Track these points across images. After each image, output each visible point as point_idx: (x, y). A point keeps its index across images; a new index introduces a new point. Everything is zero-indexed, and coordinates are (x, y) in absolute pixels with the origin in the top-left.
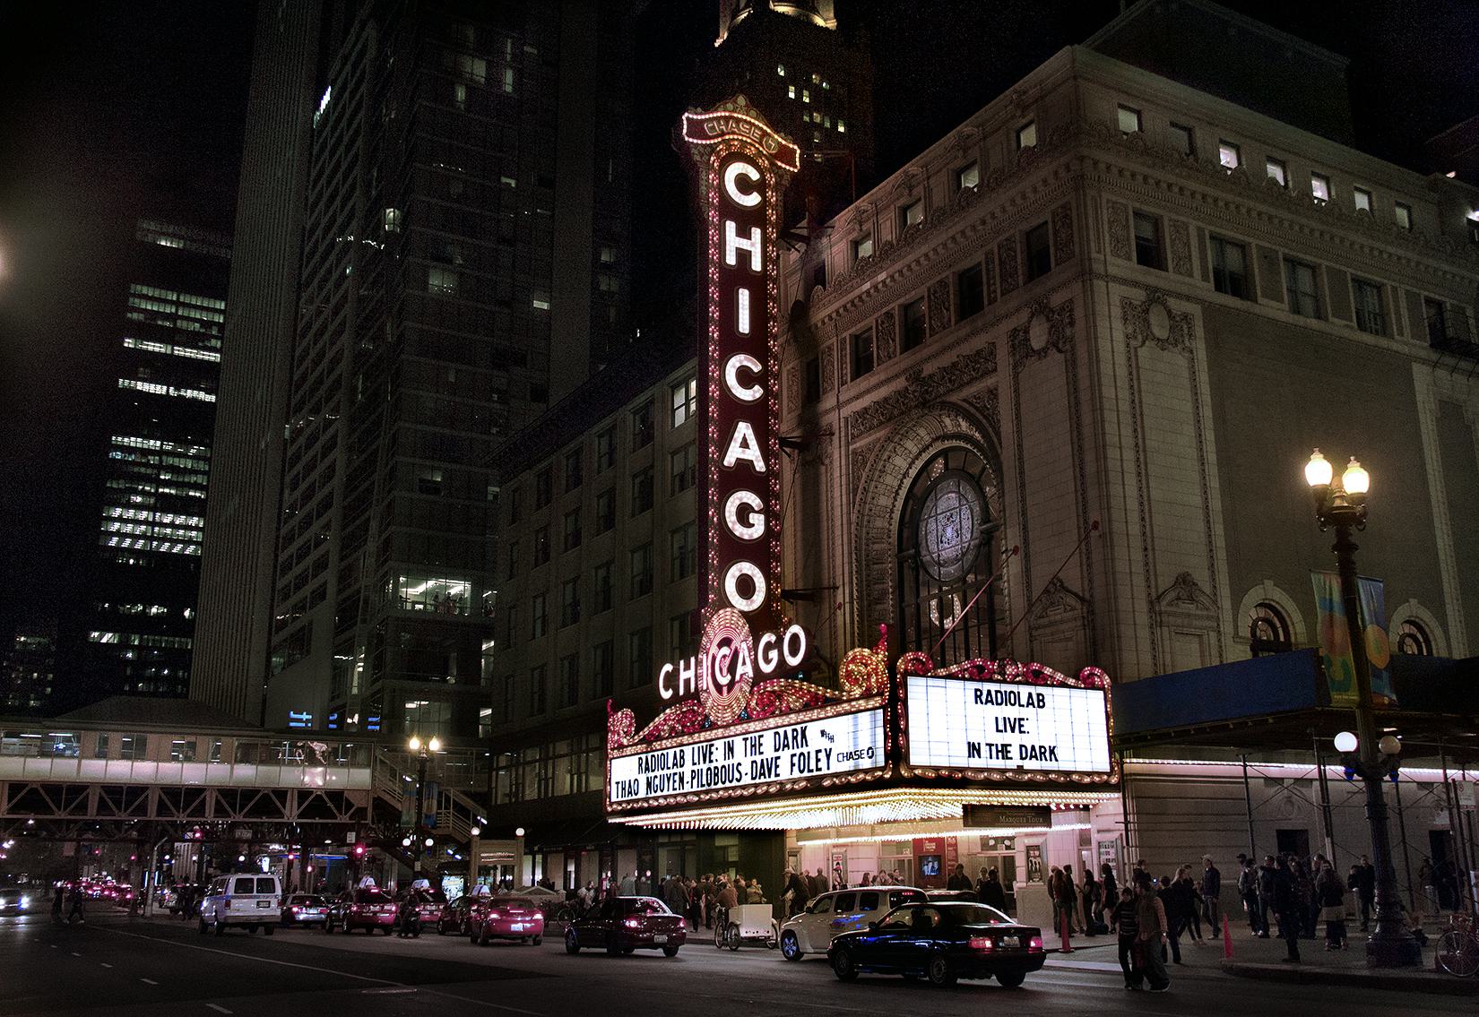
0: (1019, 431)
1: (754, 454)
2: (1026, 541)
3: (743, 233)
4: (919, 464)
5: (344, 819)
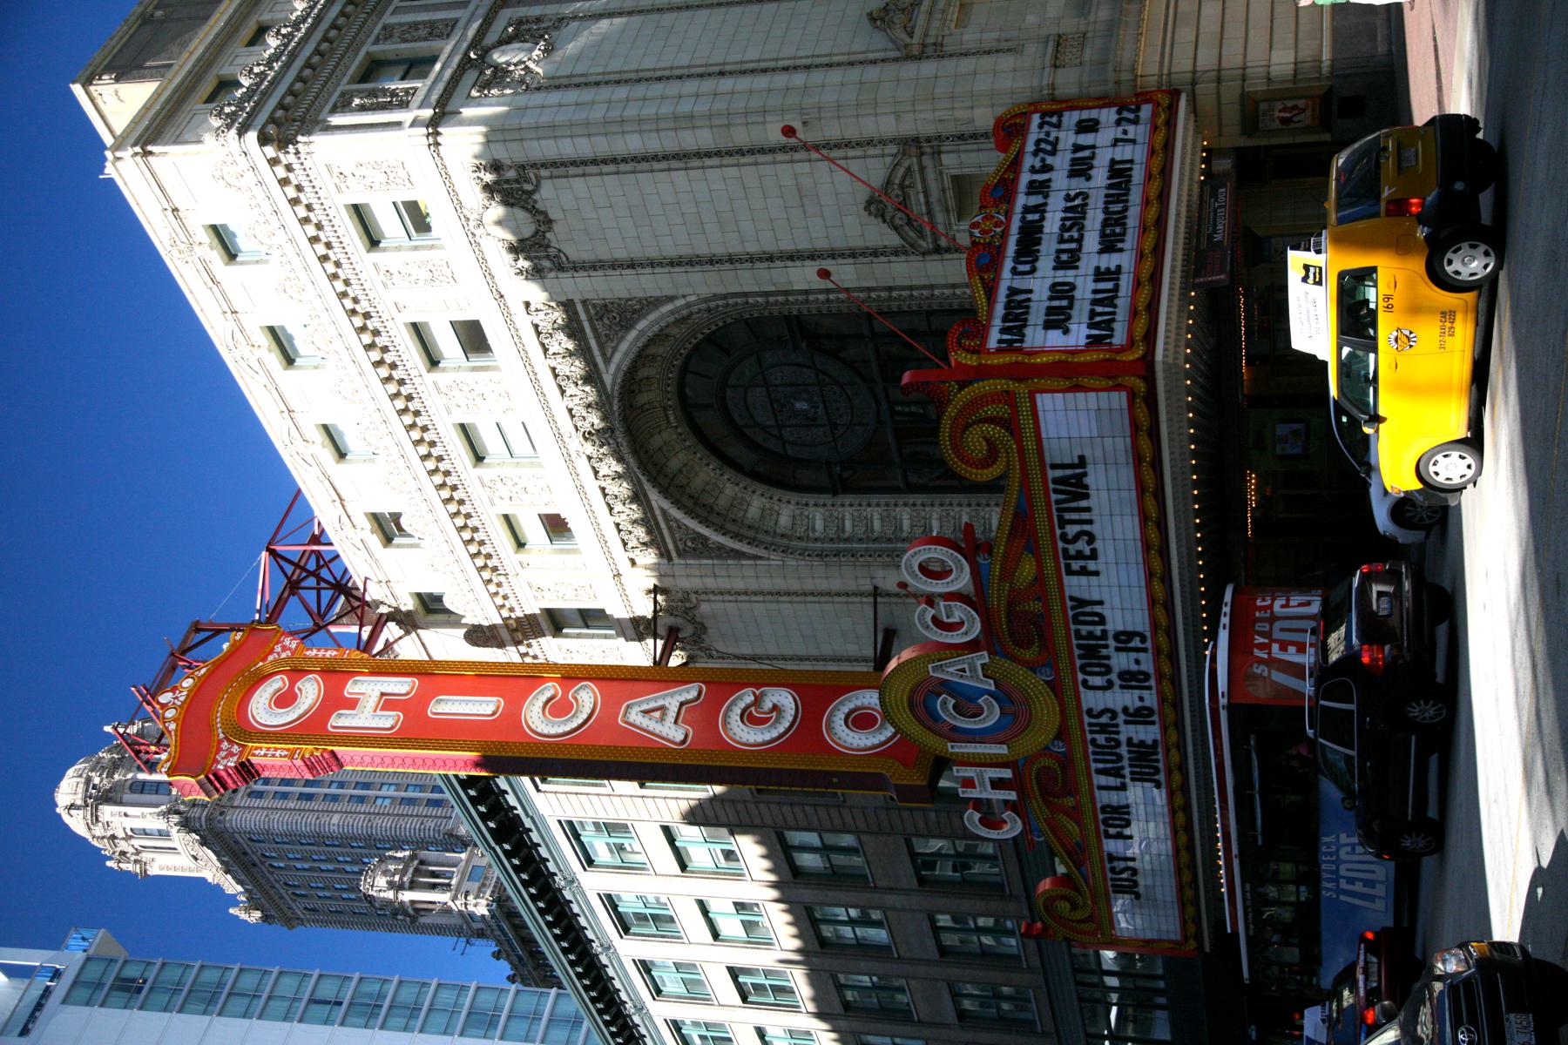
0: (652, 264)
3: (352, 704)
4: (702, 452)
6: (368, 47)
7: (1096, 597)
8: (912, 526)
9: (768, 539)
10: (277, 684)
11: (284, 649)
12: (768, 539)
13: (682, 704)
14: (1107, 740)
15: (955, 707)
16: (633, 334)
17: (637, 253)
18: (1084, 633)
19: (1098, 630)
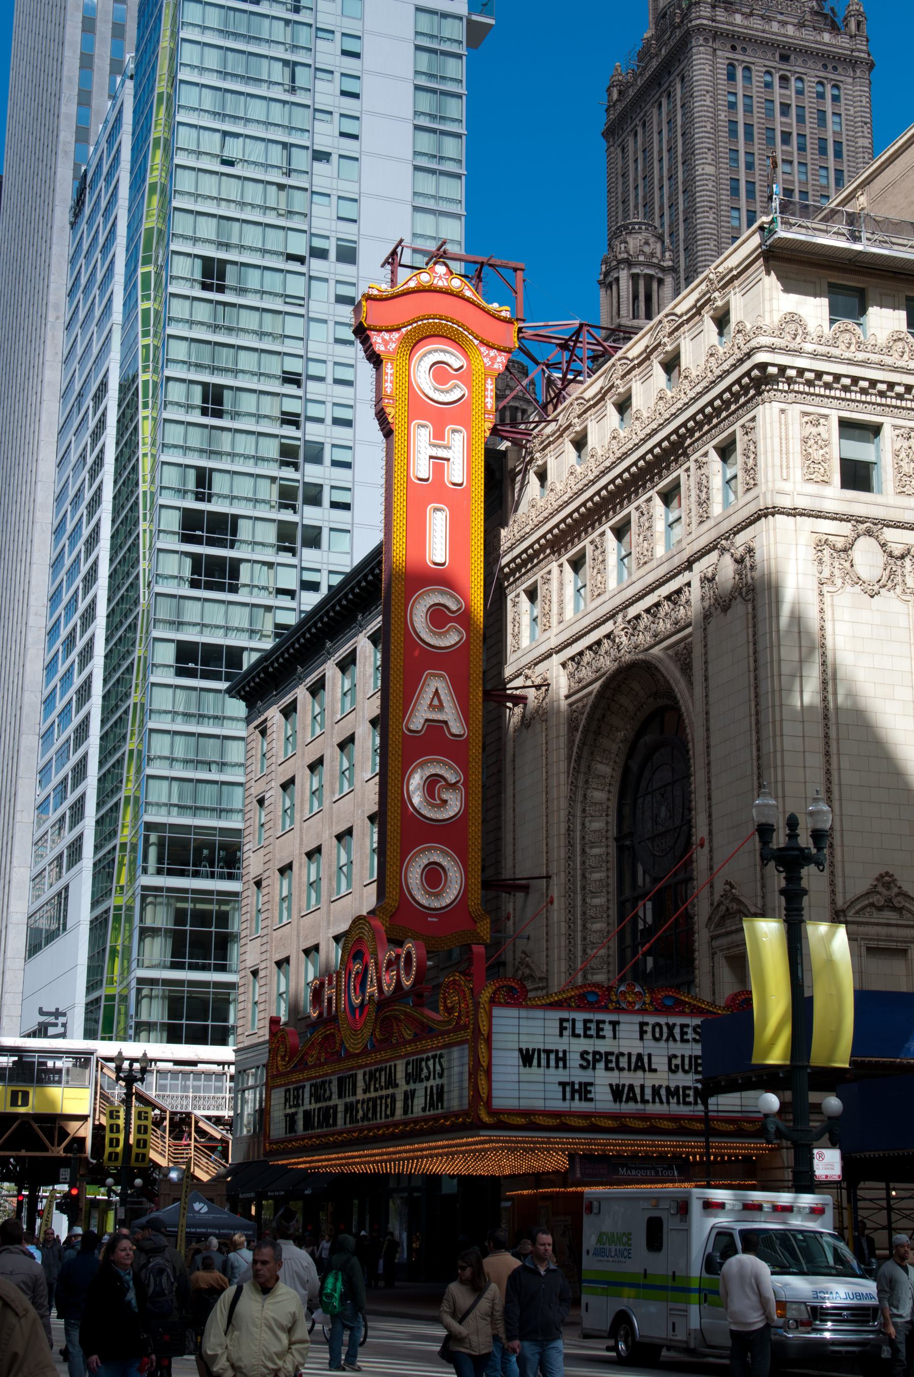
2: (710, 833)
3: (439, 434)
5: (59, 1151)
6: (888, 423)
8: (596, 907)
9: (580, 784)
10: (455, 360)
11: (493, 359)
12: (581, 784)
13: (446, 722)
16: (677, 674)
17: (712, 683)
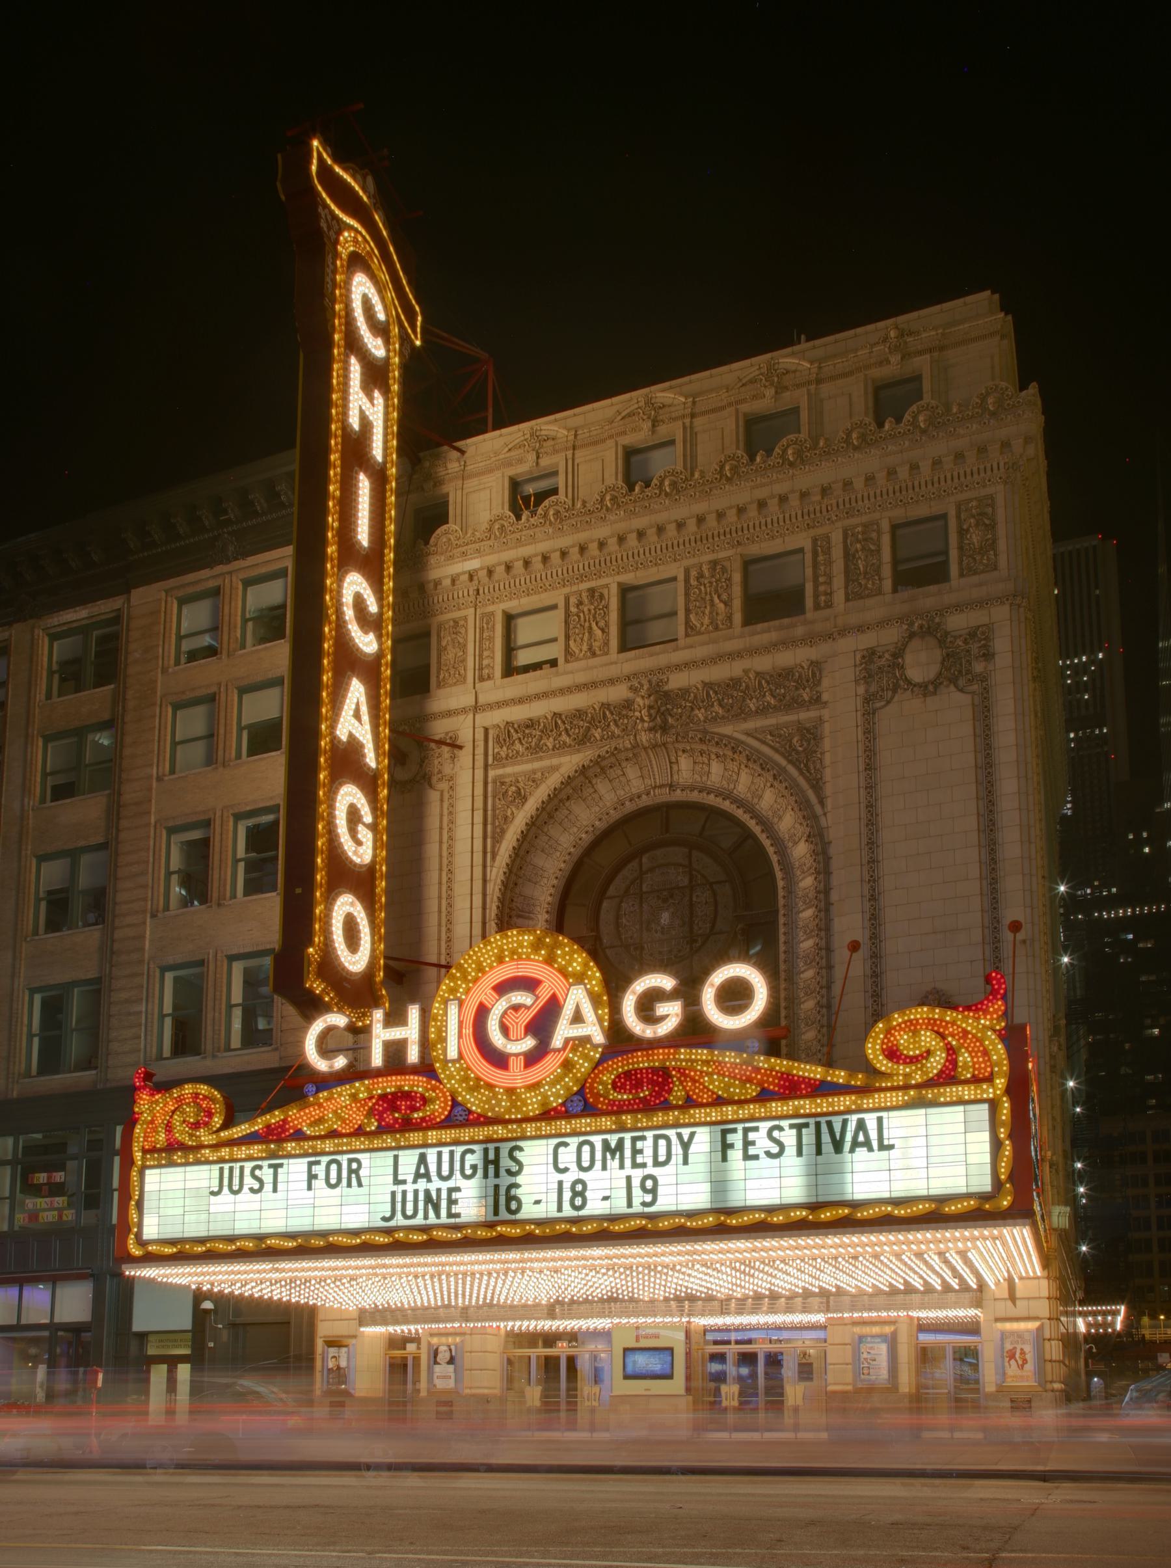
0: (870, 788)
1: (364, 734)
7: (691, 1158)
14: (474, 1167)
15: (516, 1008)
18: (639, 1145)
19: (647, 1157)
